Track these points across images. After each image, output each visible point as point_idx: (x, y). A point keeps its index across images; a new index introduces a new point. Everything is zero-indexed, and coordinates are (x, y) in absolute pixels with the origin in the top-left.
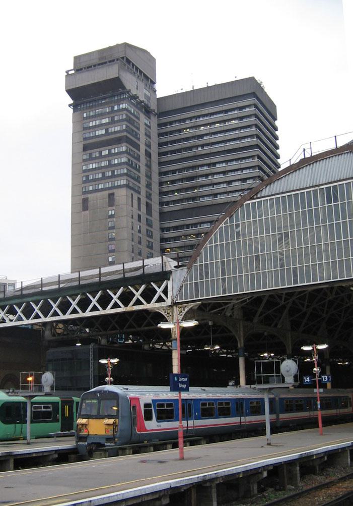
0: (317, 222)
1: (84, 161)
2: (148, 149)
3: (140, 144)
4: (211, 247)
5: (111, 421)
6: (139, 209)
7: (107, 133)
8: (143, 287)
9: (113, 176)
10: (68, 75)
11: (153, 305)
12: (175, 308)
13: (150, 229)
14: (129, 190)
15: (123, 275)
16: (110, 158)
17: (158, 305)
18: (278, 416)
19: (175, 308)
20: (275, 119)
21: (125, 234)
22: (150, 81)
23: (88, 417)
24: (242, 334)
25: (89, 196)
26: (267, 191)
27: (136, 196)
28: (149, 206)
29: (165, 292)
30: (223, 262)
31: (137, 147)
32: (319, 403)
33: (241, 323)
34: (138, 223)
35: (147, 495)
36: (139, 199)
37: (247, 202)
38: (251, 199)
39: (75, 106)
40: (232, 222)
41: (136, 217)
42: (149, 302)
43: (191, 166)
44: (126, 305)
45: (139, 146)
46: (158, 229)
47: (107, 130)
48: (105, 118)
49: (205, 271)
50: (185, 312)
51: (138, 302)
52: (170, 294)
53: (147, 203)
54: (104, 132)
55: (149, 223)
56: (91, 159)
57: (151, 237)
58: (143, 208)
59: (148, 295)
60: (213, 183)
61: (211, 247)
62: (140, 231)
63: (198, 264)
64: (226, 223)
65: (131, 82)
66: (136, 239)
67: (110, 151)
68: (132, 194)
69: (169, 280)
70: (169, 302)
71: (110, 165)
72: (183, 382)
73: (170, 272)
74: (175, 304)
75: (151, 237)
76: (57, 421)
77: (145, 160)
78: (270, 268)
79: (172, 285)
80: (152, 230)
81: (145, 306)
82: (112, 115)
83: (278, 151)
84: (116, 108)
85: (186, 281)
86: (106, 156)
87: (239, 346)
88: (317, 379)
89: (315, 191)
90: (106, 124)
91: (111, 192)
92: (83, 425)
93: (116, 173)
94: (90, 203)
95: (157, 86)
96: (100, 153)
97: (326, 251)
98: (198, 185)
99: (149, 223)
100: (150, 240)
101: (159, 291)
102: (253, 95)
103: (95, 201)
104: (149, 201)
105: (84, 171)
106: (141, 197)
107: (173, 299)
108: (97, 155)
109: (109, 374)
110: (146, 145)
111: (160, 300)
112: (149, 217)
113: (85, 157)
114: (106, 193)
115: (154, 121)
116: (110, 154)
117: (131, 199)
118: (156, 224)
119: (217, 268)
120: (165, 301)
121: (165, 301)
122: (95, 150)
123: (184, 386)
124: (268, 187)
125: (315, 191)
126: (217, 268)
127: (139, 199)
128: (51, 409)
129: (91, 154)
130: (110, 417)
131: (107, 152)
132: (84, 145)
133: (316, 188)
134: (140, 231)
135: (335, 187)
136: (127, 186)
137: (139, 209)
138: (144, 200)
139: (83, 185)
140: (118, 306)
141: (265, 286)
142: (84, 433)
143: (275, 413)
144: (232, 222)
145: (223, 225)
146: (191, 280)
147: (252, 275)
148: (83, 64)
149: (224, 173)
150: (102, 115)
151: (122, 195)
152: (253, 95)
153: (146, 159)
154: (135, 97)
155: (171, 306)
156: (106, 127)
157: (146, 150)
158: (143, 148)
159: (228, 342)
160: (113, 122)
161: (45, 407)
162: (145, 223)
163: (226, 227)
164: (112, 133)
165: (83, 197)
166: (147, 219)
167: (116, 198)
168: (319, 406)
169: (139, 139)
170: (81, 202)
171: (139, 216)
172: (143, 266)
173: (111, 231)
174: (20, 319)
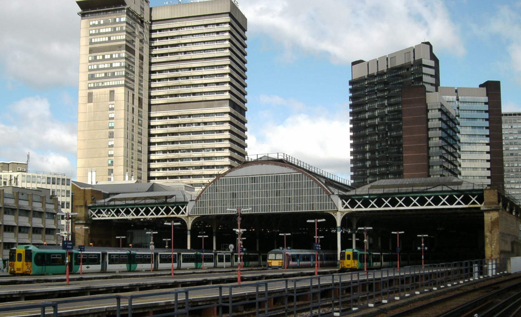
1: (90, 61)
2: (141, 53)
3: (136, 50)
4: (205, 194)
6: (133, 103)
7: (110, 40)
8: (175, 208)
9: (113, 76)
11: (179, 215)
12: (189, 217)
14: (126, 88)
16: (111, 62)
17: (182, 215)
19: (189, 217)
20: (245, 30)
25: (94, 91)
27: (131, 92)
28: (140, 100)
29: (185, 210)
30: (210, 201)
31: (134, 53)
36: (133, 95)
37: (221, 178)
38: (223, 177)
40: (214, 185)
42: (178, 214)
43: (175, 68)
44: (167, 214)
45: (134, 51)
47: (109, 38)
48: (108, 28)
50: (193, 219)
51: (173, 213)
52: (187, 211)
53: (139, 98)
54: (107, 39)
56: (95, 60)
57: (141, 125)
59: (178, 211)
60: (192, 83)
61: (205, 194)
63: (200, 200)
64: (212, 185)
67: (111, 55)
68: (128, 92)
69: (187, 205)
70: (187, 215)
71: (111, 67)
73: (187, 203)
74: (189, 216)
76: (99, 264)
77: (139, 62)
79: (189, 207)
81: (176, 215)
82: (114, 26)
83: (246, 65)
84: (117, 20)
86: (108, 60)
87: (214, 231)
90: (108, 33)
91: (112, 89)
93: (116, 75)
94: (94, 97)
96: (104, 56)
98: (180, 84)
101: (183, 210)
103: (98, 96)
104: (140, 96)
105: (90, 70)
106: (135, 94)
107: (188, 214)
108: (101, 57)
109: (167, 244)
110: (140, 50)
111: (183, 213)
112: (140, 109)
113: (90, 59)
114: (108, 90)
116: (112, 58)
117: (127, 95)
119: (207, 203)
120: (184, 214)
121: (184, 214)
122: (99, 54)
124: (230, 173)
126: (207, 203)
127: (133, 95)
128: (127, 258)
129: (96, 57)
131: (109, 57)
132: (90, 48)
133: (247, 177)
137: (133, 103)
138: (137, 96)
139: (89, 82)
140: (163, 214)
144: (214, 185)
146: (196, 206)
147: (221, 207)
150: (106, 24)
151: (120, 92)
153: (139, 61)
154: (133, 13)
155: (188, 217)
156: (109, 35)
157: (140, 54)
158: (137, 52)
159: (209, 232)
160: (114, 31)
161: (94, 256)
163: (212, 187)
164: (114, 41)
165: (89, 91)
167: (116, 95)
169: (134, 46)
170: (87, 95)
171: (133, 109)
173: (111, 121)
174: (113, 216)
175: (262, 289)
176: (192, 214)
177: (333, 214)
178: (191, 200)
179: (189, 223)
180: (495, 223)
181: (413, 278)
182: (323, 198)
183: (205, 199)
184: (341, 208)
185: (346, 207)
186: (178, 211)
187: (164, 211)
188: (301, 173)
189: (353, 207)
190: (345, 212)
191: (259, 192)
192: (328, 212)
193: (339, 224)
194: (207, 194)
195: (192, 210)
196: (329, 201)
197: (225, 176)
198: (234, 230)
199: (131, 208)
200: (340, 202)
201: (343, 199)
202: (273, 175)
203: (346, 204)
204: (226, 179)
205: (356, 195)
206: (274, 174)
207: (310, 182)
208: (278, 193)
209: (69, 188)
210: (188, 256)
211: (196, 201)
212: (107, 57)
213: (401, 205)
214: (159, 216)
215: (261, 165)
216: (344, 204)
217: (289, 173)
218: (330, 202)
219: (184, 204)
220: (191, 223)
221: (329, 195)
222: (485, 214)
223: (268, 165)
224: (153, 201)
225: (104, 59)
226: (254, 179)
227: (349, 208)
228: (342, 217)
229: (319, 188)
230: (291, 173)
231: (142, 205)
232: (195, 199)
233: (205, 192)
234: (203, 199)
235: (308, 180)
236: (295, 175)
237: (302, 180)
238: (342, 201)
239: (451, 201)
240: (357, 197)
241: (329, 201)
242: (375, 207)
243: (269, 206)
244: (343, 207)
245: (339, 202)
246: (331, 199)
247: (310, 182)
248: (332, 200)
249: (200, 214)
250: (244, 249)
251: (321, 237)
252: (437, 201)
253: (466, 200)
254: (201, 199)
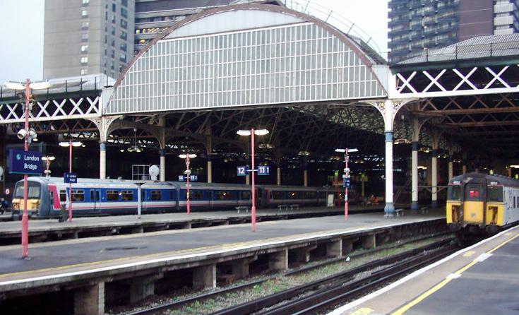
0: (207, 62)
4: (131, 74)
5: (36, 201)
8: (81, 100)
12: (103, 118)
13: (124, 19)
15: (65, 88)
18: (177, 203)
21: (98, 24)
23: (21, 198)
24: (164, 138)
26: (173, 34)
29: (97, 105)
32: (188, 194)
33: (164, 129)
34: (112, 13)
35: (34, 232)
37: (159, 41)
38: (162, 39)
40: (147, 55)
41: (110, 7)
46: (133, 20)
49: (127, 92)
50: (110, 122)
51: (76, 112)
55: (124, 14)
57: (125, 27)
59: (85, 107)
61: (131, 74)
62: (114, 21)
66: (110, 30)
70: (99, 114)
72: (72, 178)
73: (101, 91)
75: (125, 27)
78: (172, 94)
80: (126, 20)
81: (82, 116)
85: (111, 98)
87: (161, 148)
88: (188, 178)
89: (207, 38)
92: (16, 203)
97: (211, 84)
99: (124, 14)
100: (124, 30)
101: (93, 104)
109: (48, 168)
111: (93, 112)
112: (124, 7)
118: (131, 14)
119: (135, 90)
120: (95, 112)
121: (95, 112)
123: (74, 180)
125: (207, 38)
130: (34, 198)
134: (114, 21)
135: (221, 37)
141: (167, 108)
142: (16, 208)
143: (174, 200)
144: (147, 55)
145: (141, 57)
146: (116, 98)
162: (120, 13)
163: (143, 59)
166: (122, 9)
168: (188, 197)
171: (114, 6)
172: (82, 83)
176: (108, 111)
177: (376, 106)
178: (107, 87)
179: (103, 129)
182: (357, 72)
183: (131, 83)
184: (394, 93)
185: (406, 90)
186: (85, 107)
187: (63, 108)
188: (312, 23)
189: (419, 90)
190: (402, 100)
191: (230, 64)
192: (366, 101)
194: (135, 73)
195: (109, 103)
196: (368, 78)
197: (166, 38)
199: (10, 105)
201: (398, 72)
202: (256, 30)
203: (406, 83)
204: (168, 42)
205: (428, 63)
206: (258, 28)
207: (330, 40)
208: (266, 66)
210: (129, 192)
211: (115, 87)
215: (233, 13)
216: (400, 83)
217: (288, 24)
218: (371, 81)
219: (95, 93)
220: (106, 130)
221: (370, 67)
223: (247, 11)
226: (219, 40)
227: (411, 92)
228: (397, 110)
229: (349, 51)
230: (291, 24)
232: (113, 85)
233: (131, 70)
234: (128, 84)
235: (325, 36)
236: (298, 27)
237: (314, 37)
238: (397, 77)
240: (428, 68)
241: (368, 78)
242: (471, 88)
243: (248, 92)
244: (398, 89)
245: (388, 79)
246: (373, 73)
247: (330, 40)
248: (375, 76)
249: (122, 113)
250: (193, 178)
251: (350, 151)
254: (124, 84)
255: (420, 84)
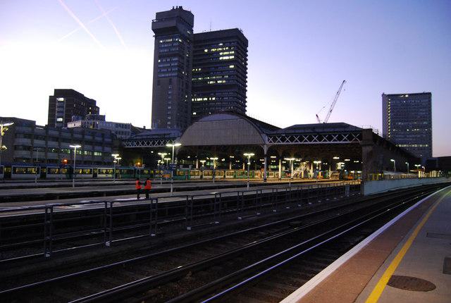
10: (153, 23)
22: (191, 25)
39: (156, 37)
58: (185, 86)
65: (181, 28)
95: (194, 29)
102: (237, 37)
115: (192, 45)
136: (178, 76)
148: (160, 16)
149: (222, 72)
152: (237, 37)
175: (259, 192)
180: (370, 154)
181: (299, 194)
184: (267, 143)
185: (271, 142)
193: (265, 153)
198: (159, 154)
200: (267, 139)
209: (129, 130)
212: (168, 60)
213: (306, 141)
214: (160, 146)
222: (363, 148)
224: (157, 137)
225: (167, 62)
231: (151, 139)
239: (340, 138)
252: (330, 138)
253: (350, 138)
255: (275, 140)
